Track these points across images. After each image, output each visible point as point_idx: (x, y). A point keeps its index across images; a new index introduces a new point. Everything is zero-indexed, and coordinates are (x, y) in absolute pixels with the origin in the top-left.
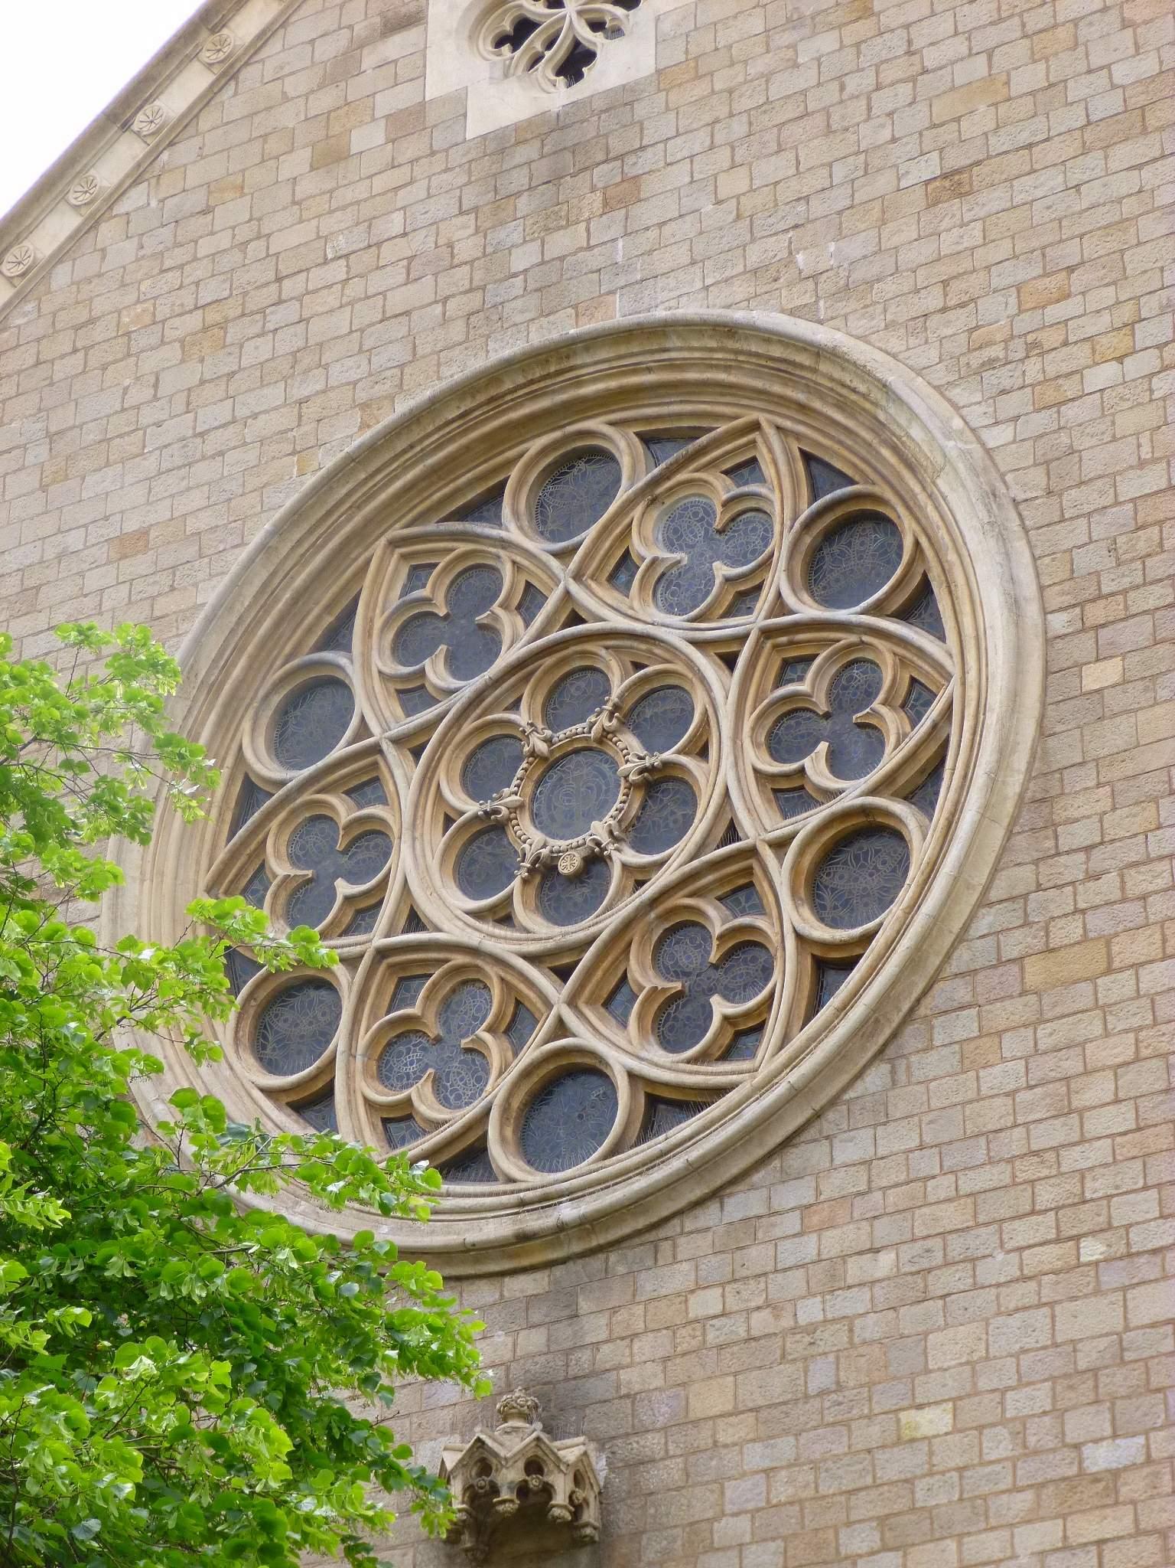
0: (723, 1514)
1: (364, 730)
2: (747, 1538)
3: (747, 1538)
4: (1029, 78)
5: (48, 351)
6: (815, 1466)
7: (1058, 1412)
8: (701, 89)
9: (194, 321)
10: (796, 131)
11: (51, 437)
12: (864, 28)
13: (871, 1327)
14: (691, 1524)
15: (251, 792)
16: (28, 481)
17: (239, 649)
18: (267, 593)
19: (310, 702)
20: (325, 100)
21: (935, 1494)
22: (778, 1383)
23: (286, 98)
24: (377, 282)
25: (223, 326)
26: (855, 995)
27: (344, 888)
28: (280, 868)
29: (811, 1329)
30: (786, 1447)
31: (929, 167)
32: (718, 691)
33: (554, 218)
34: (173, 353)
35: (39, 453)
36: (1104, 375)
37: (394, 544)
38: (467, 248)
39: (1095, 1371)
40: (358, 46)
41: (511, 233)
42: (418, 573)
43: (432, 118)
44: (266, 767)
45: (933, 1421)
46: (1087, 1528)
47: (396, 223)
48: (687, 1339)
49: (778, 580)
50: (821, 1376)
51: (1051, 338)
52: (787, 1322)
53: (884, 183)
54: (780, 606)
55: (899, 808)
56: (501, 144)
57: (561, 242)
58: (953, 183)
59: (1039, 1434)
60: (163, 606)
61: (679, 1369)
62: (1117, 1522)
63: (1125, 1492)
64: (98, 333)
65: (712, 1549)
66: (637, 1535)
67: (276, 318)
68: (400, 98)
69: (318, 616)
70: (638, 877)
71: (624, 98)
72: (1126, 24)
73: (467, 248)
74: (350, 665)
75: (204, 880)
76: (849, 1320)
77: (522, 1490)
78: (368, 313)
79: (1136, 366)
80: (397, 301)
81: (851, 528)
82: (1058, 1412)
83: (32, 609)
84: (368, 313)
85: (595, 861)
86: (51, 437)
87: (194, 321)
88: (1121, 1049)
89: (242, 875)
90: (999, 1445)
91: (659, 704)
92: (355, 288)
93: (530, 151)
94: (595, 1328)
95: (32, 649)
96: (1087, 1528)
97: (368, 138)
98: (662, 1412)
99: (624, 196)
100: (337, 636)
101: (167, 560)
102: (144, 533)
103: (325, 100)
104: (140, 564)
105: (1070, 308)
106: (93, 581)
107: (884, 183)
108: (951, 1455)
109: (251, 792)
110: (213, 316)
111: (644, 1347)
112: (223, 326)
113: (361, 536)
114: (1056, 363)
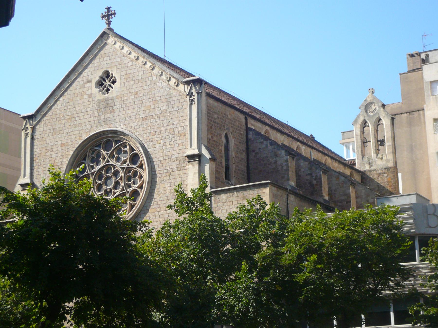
1: (88, 172)
4: (153, 107)
8: (120, 100)
9: (68, 117)
10: (130, 107)
11: (53, 129)
12: (137, 96)
16: (50, 134)
18: (77, 154)
20: (81, 90)
23: (76, 89)
24: (87, 116)
25: (71, 118)
26: (133, 212)
31: (142, 116)
32: (122, 173)
33: (106, 113)
34: (65, 121)
35: (52, 131)
36: (158, 145)
37: (91, 149)
38: (97, 114)
40: (84, 84)
41: (101, 114)
42: (92, 154)
43: (93, 95)
47: (89, 109)
49: (128, 162)
51: (154, 140)
53: (138, 117)
54: (128, 165)
55: (139, 190)
56: (100, 102)
57: (107, 116)
58: (145, 118)
60: (67, 153)
64: (58, 116)
67: (77, 119)
68: (89, 92)
69: (83, 157)
70: (115, 193)
71: (112, 99)
72: (162, 102)
73: (97, 114)
78: (87, 120)
79: (162, 145)
80: (90, 119)
81: (135, 158)
83: (53, 151)
84: (87, 120)
85: (111, 191)
86: (53, 129)
87: (68, 117)
88: (156, 220)
91: (116, 173)
92: (85, 117)
93: (103, 103)
95: (54, 156)
97: (86, 97)
99: (113, 112)
101: (66, 148)
102: (64, 144)
103: (81, 90)
104: (63, 148)
105: (155, 137)
107: (138, 117)
110: (70, 117)
112: (71, 118)
113: (87, 148)
114: (154, 143)
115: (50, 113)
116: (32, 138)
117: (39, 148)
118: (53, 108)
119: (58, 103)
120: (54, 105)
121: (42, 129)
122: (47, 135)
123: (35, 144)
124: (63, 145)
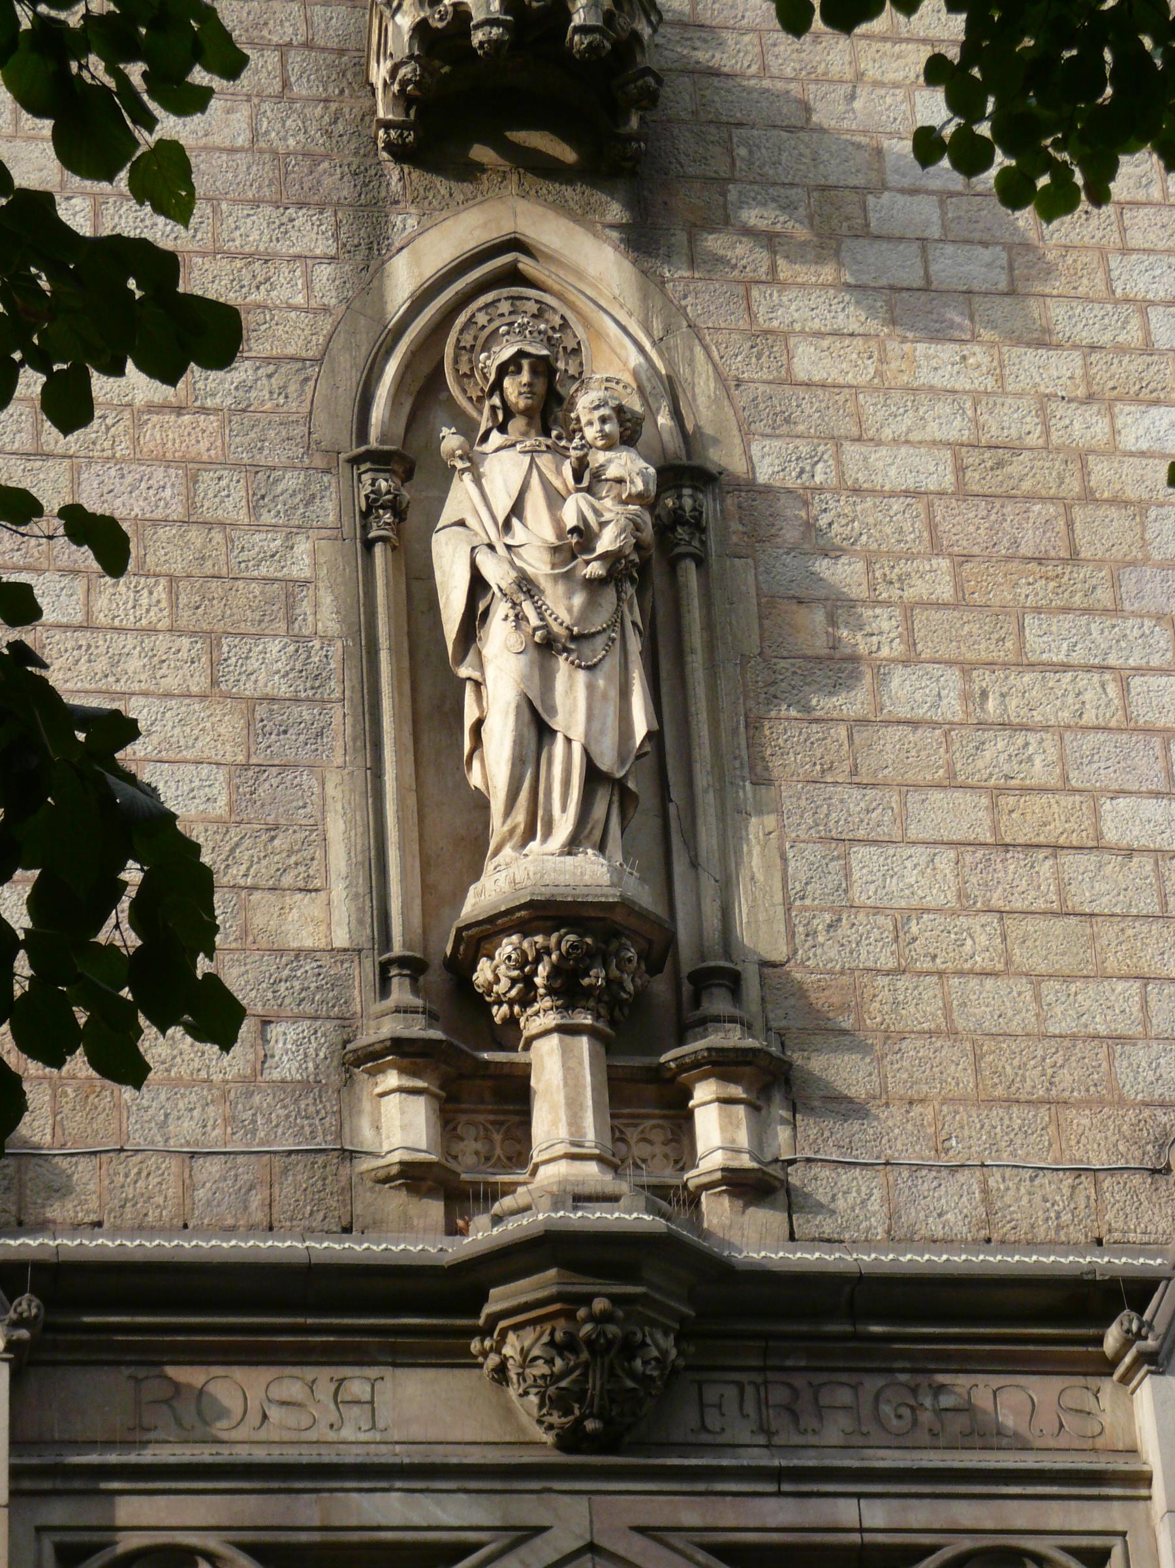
0: (884, 187)
2: (935, 232)
3: (935, 232)
14: (823, 188)
65: (865, 233)
66: (721, 183)
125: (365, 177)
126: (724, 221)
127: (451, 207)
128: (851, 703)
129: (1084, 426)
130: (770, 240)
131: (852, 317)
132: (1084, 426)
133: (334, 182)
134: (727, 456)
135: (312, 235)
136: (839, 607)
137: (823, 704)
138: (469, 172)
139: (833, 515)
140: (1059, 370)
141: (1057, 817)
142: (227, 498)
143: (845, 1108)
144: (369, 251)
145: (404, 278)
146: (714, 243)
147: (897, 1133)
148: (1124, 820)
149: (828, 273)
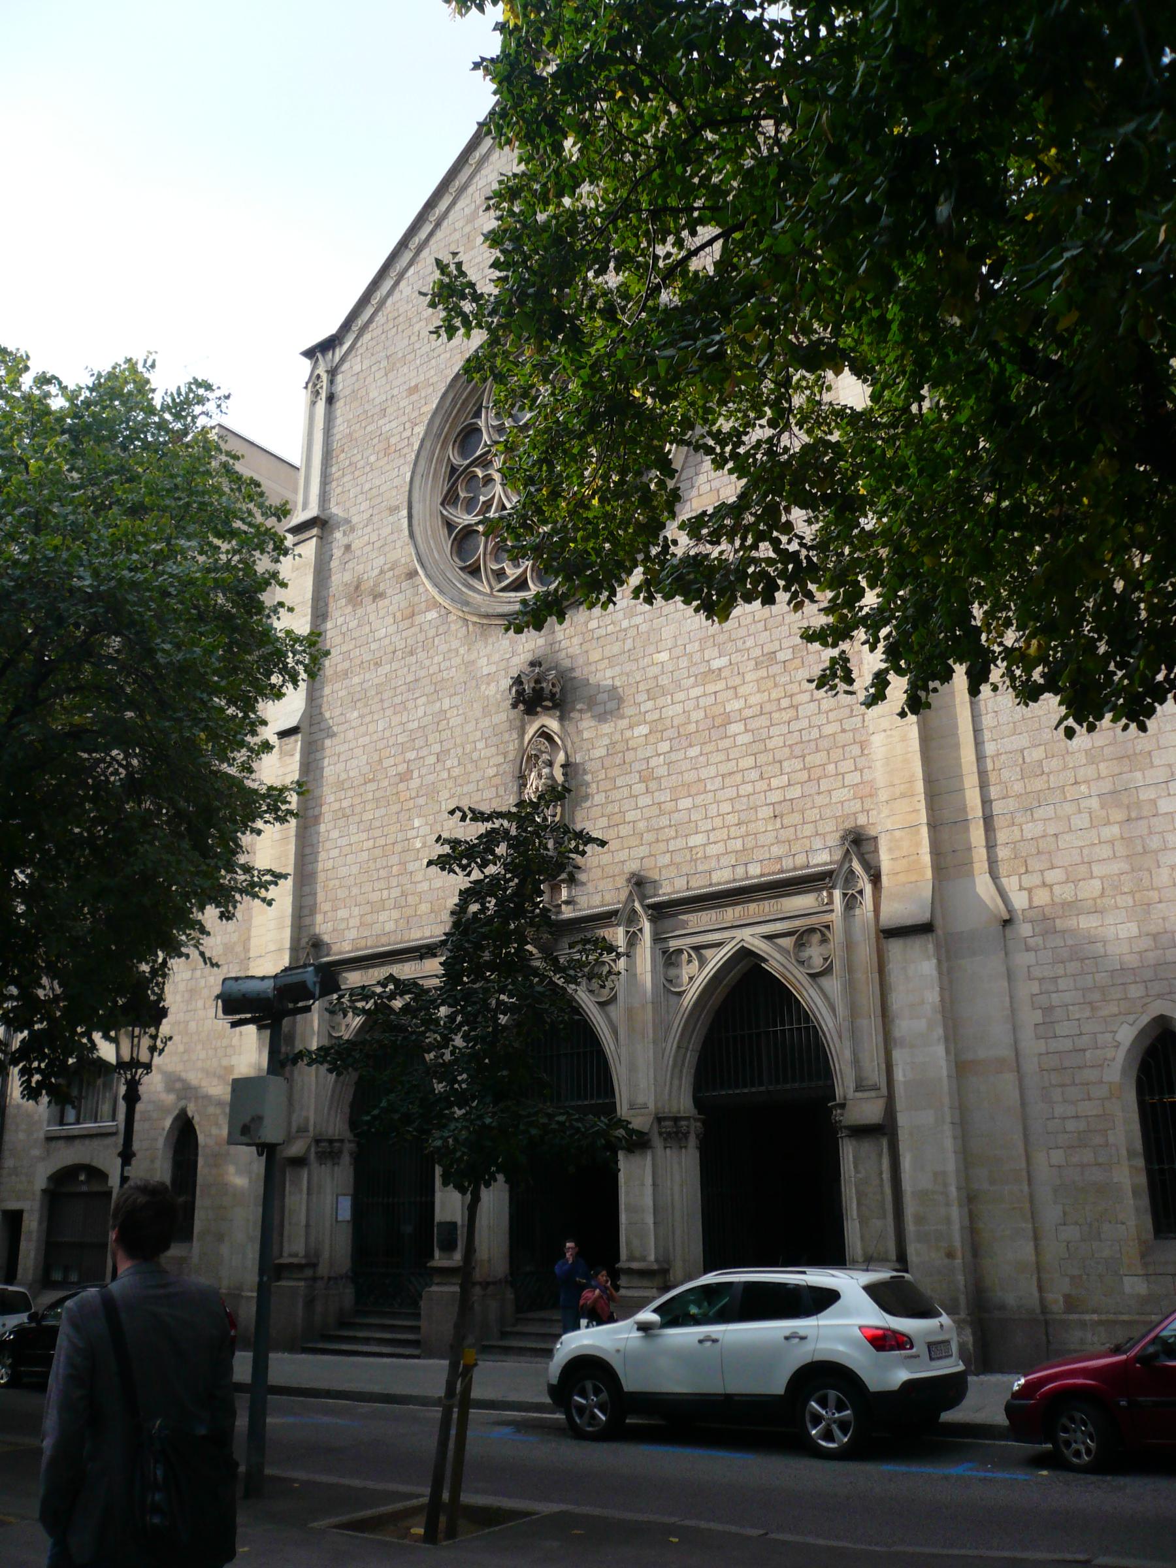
5: (386, 328)
6: (628, 675)
7: (702, 650)
11: (388, 357)
13: (644, 628)
15: (453, 469)
17: (447, 421)
19: (469, 435)
21: (664, 681)
22: (616, 648)
23: (455, 230)
27: (482, 499)
28: (462, 495)
29: (625, 630)
30: (618, 669)
35: (384, 363)
39: (713, 636)
44: (457, 460)
45: (664, 656)
46: (711, 688)
48: (588, 636)
50: (629, 644)
52: (618, 628)
59: (697, 658)
61: (585, 647)
62: (721, 685)
63: (723, 675)
64: (401, 319)
65: (596, 704)
74: (481, 423)
75: (440, 500)
76: (638, 626)
77: (534, 689)
82: (702, 650)
86: (388, 357)
89: (450, 499)
90: (683, 663)
94: (560, 635)
96: (711, 688)
98: (581, 661)
100: (477, 415)
102: (416, 386)
104: (414, 397)
106: (402, 404)
108: (670, 667)
109: (453, 469)
111: (575, 641)
115: (380, 319)
116: (331, 399)
117: (348, 421)
118: (389, 301)
119: (403, 284)
120: (390, 293)
121: (357, 368)
122: (370, 379)
123: (338, 413)
124: (414, 390)
125: (522, 720)
126: (573, 710)
127: (534, 721)
128: (588, 804)
129: (628, 734)
130: (581, 711)
131: (593, 723)
132: (628, 734)
133: (518, 723)
134: (572, 760)
135: (515, 736)
136: (587, 784)
137: (584, 805)
138: (536, 714)
139: (588, 767)
140: (625, 722)
141: (617, 819)
142: (501, 791)
143: (583, 884)
144: (522, 733)
145: (527, 738)
146: (572, 715)
147: (590, 887)
148: (630, 816)
149: (589, 714)
